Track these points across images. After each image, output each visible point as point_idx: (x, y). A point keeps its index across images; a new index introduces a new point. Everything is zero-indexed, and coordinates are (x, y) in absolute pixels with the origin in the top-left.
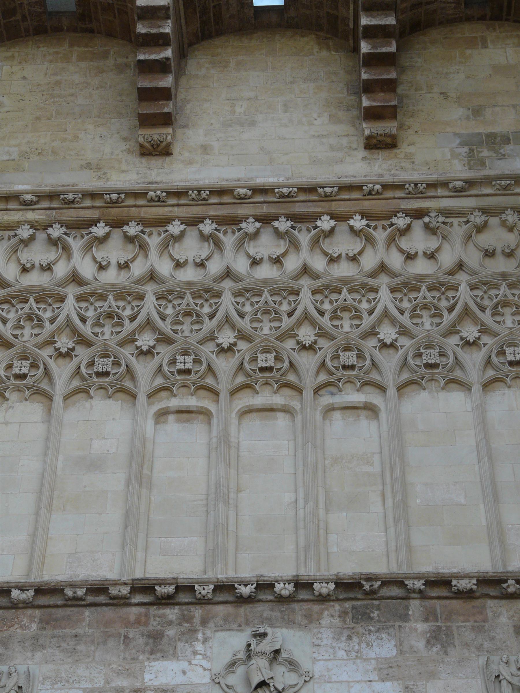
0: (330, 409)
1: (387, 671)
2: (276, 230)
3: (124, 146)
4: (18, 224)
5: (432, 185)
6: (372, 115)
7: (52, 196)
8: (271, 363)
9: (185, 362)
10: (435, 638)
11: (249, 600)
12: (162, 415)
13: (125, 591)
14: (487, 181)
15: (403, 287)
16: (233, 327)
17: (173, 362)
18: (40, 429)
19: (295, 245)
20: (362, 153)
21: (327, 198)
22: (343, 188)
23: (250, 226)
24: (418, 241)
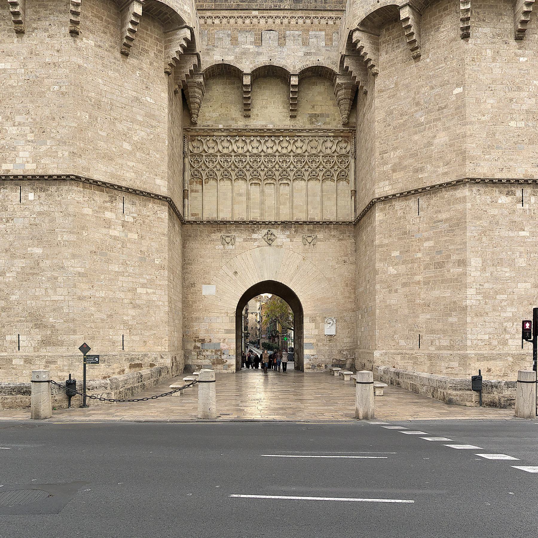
0: (281, 184)
1: (288, 237)
3: (240, 113)
4: (220, 136)
5: (302, 130)
6: (291, 110)
7: (227, 130)
9: (255, 173)
10: (295, 231)
20: (289, 118)
21: (282, 132)
22: (285, 130)
23: (267, 138)
24: (299, 144)
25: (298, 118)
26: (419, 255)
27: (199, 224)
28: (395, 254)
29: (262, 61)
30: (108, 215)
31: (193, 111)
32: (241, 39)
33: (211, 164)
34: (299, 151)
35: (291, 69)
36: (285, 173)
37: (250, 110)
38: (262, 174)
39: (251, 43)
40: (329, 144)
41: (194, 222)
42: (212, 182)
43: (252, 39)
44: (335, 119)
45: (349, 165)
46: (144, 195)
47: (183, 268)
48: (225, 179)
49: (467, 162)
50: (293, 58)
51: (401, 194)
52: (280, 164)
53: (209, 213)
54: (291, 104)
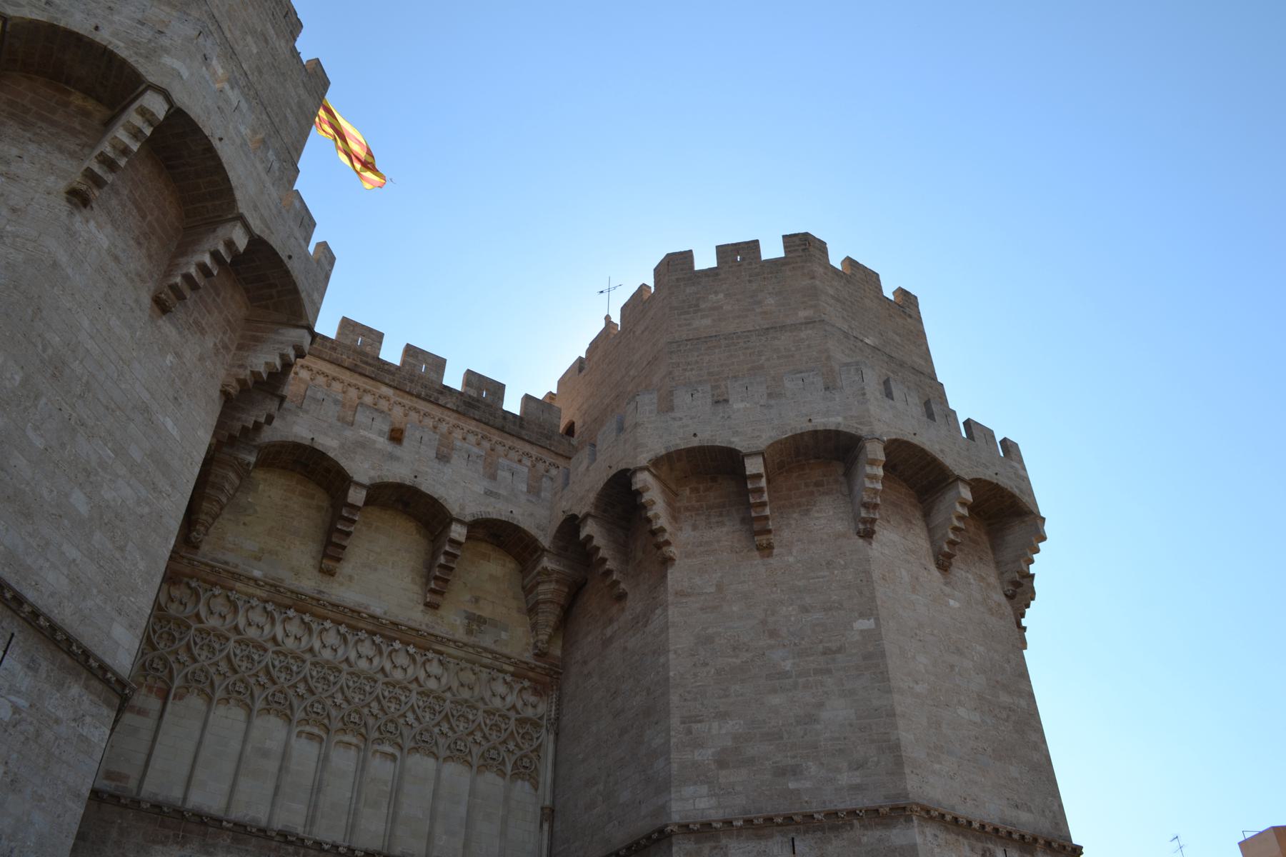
2: (373, 642)
6: (433, 591)
8: (357, 720)
11: (327, 851)
12: (299, 734)
13: (274, 834)
14: (473, 647)
15: (424, 694)
16: (343, 693)
17: (312, 706)
18: (243, 726)
19: (381, 653)
20: (421, 607)
23: (363, 635)
24: (434, 668)
25: (441, 612)
27: (126, 806)
29: (399, 472)
31: (203, 517)
32: (361, 417)
33: (205, 653)
34: (432, 684)
35: (454, 510)
36: (391, 727)
37: (339, 560)
38: (334, 712)
39: (380, 433)
40: (501, 688)
41: (111, 795)
42: (196, 701)
44: (516, 640)
45: (540, 745)
46: (70, 653)
48: (232, 701)
49: (907, 771)
50: (463, 490)
51: (749, 822)
52: (384, 702)
54: (436, 578)
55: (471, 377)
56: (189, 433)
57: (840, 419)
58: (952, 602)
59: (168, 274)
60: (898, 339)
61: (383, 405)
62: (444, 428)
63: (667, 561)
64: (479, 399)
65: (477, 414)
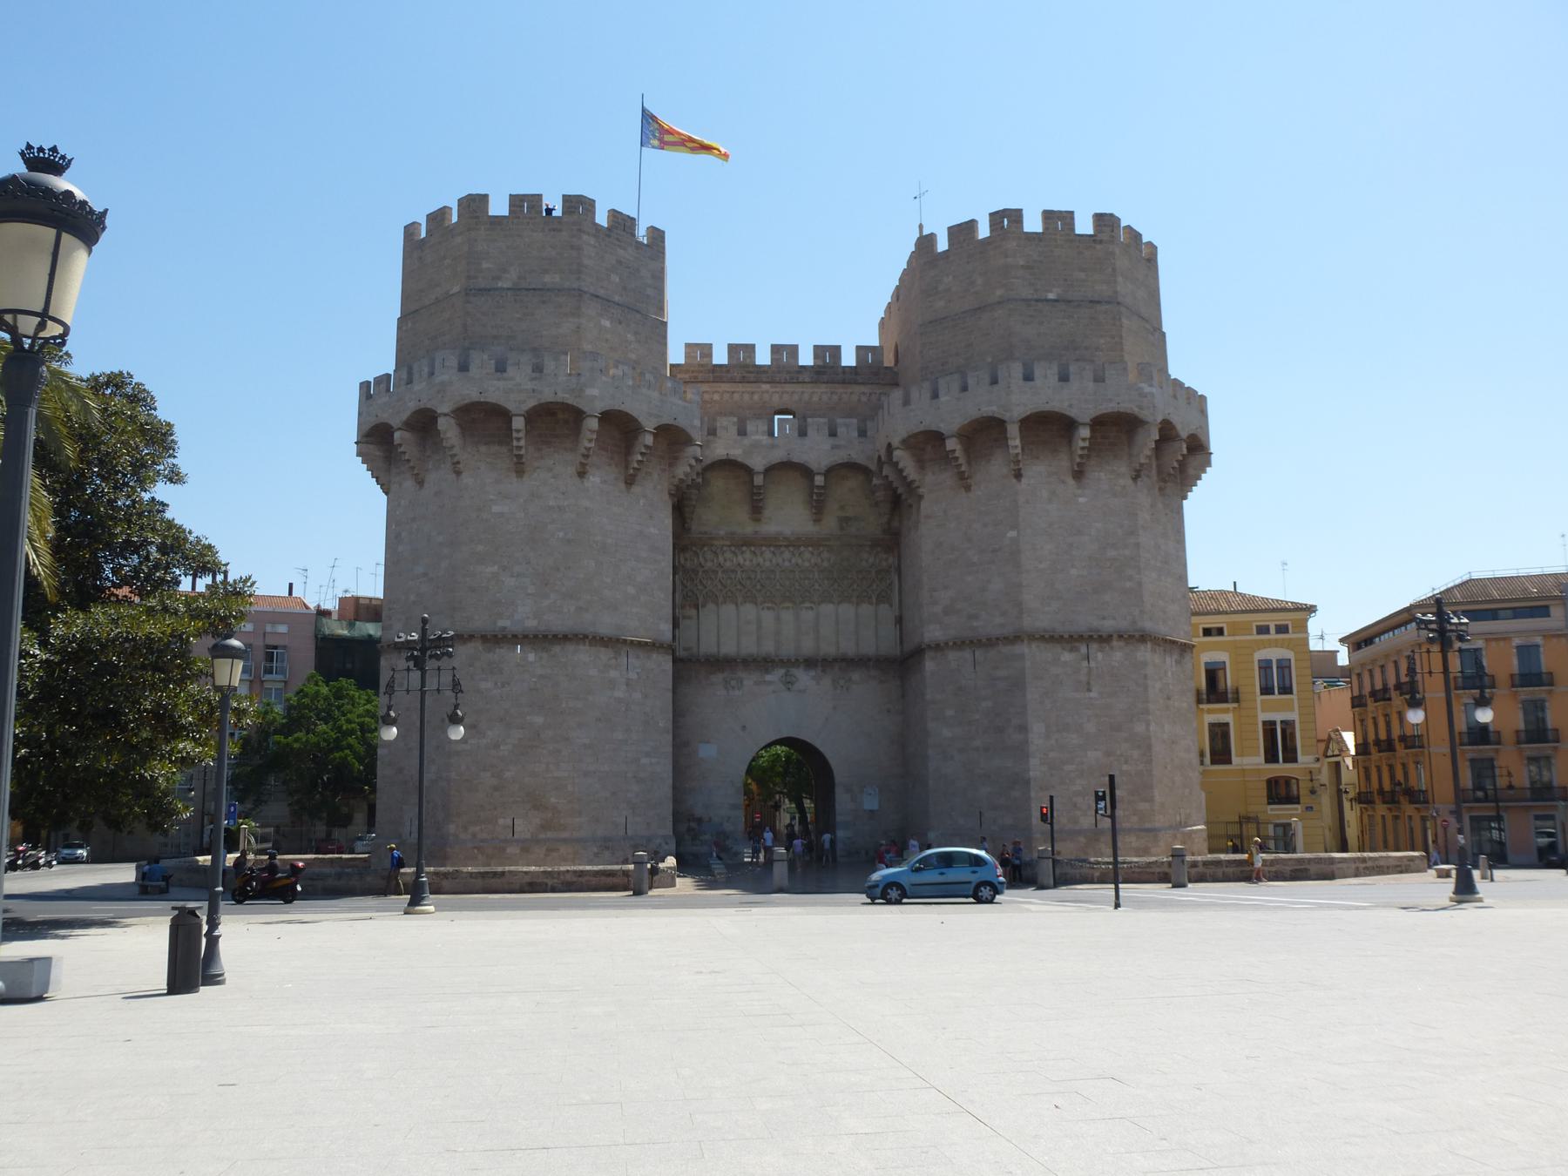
24: (825, 555)
26: (977, 717)
28: (950, 713)
29: (778, 456)
30: (613, 674)
32: (750, 427)
34: (825, 564)
35: (814, 466)
42: (711, 606)
43: (766, 428)
47: (675, 721)
50: (817, 451)
53: (708, 646)
55: (819, 351)
56: (662, 526)
57: (994, 408)
58: (1081, 500)
59: (627, 467)
60: (1082, 275)
61: (766, 396)
62: (806, 397)
63: (921, 497)
64: (825, 366)
65: (825, 378)
